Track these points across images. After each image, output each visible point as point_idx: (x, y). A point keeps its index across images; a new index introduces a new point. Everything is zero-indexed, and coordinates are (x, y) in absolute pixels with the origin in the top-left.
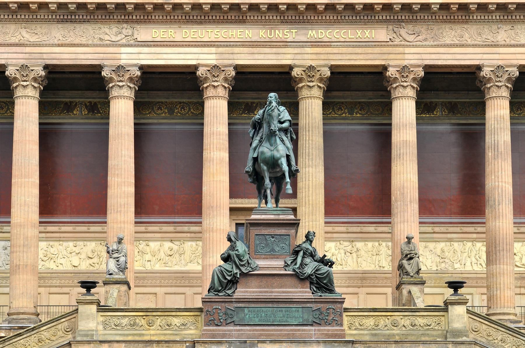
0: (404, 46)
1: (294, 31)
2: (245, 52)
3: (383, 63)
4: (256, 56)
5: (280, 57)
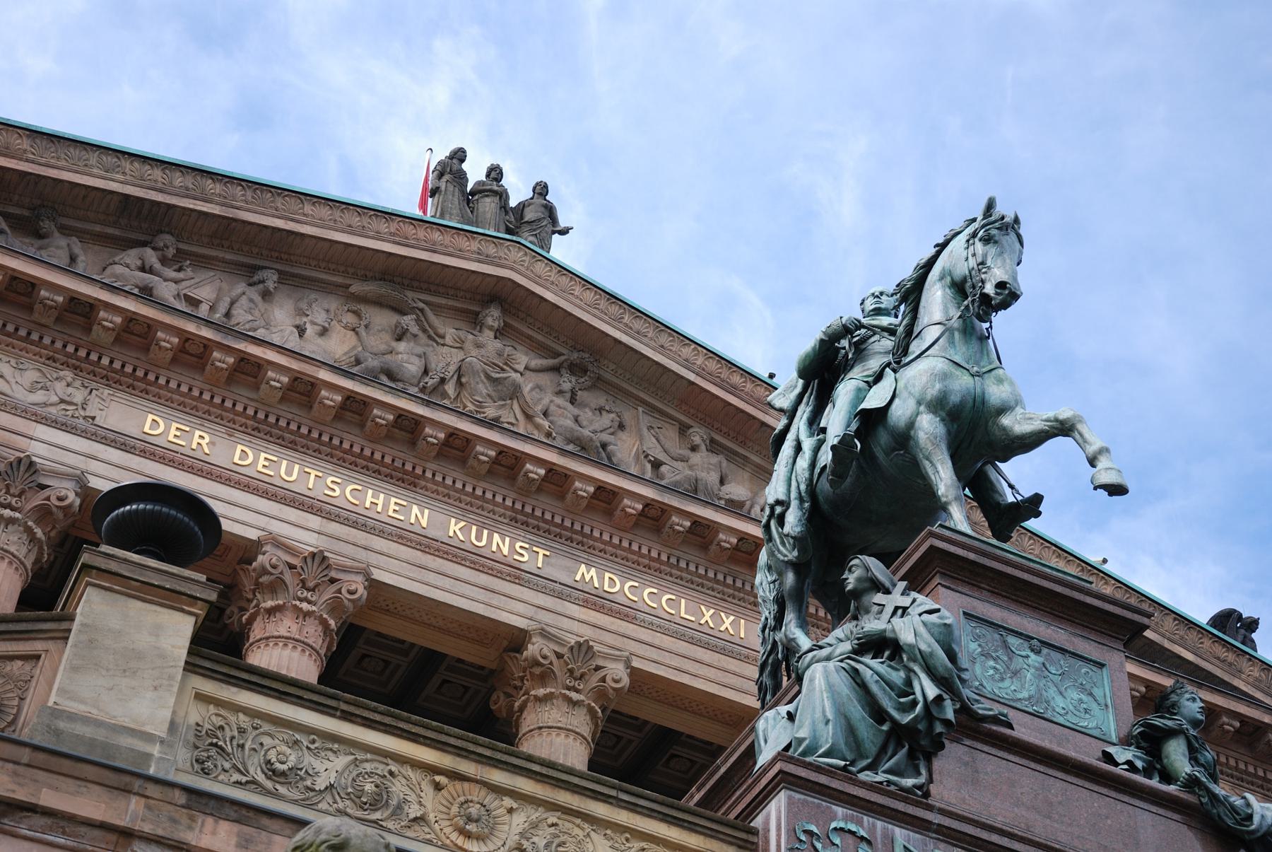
2: (403, 557)
5: (496, 600)
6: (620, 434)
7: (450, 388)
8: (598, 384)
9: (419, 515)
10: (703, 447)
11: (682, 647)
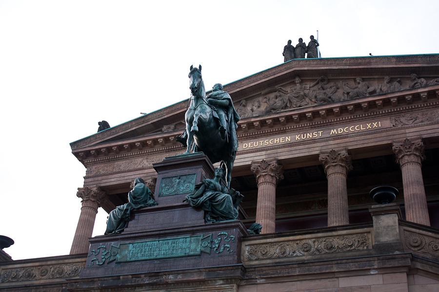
0: (405, 128)
1: (320, 132)
3: (389, 142)
4: (294, 152)
5: (310, 150)
6: (339, 90)
7: (288, 105)
8: (329, 81)
9: (288, 139)
10: (361, 82)
11: (363, 137)
